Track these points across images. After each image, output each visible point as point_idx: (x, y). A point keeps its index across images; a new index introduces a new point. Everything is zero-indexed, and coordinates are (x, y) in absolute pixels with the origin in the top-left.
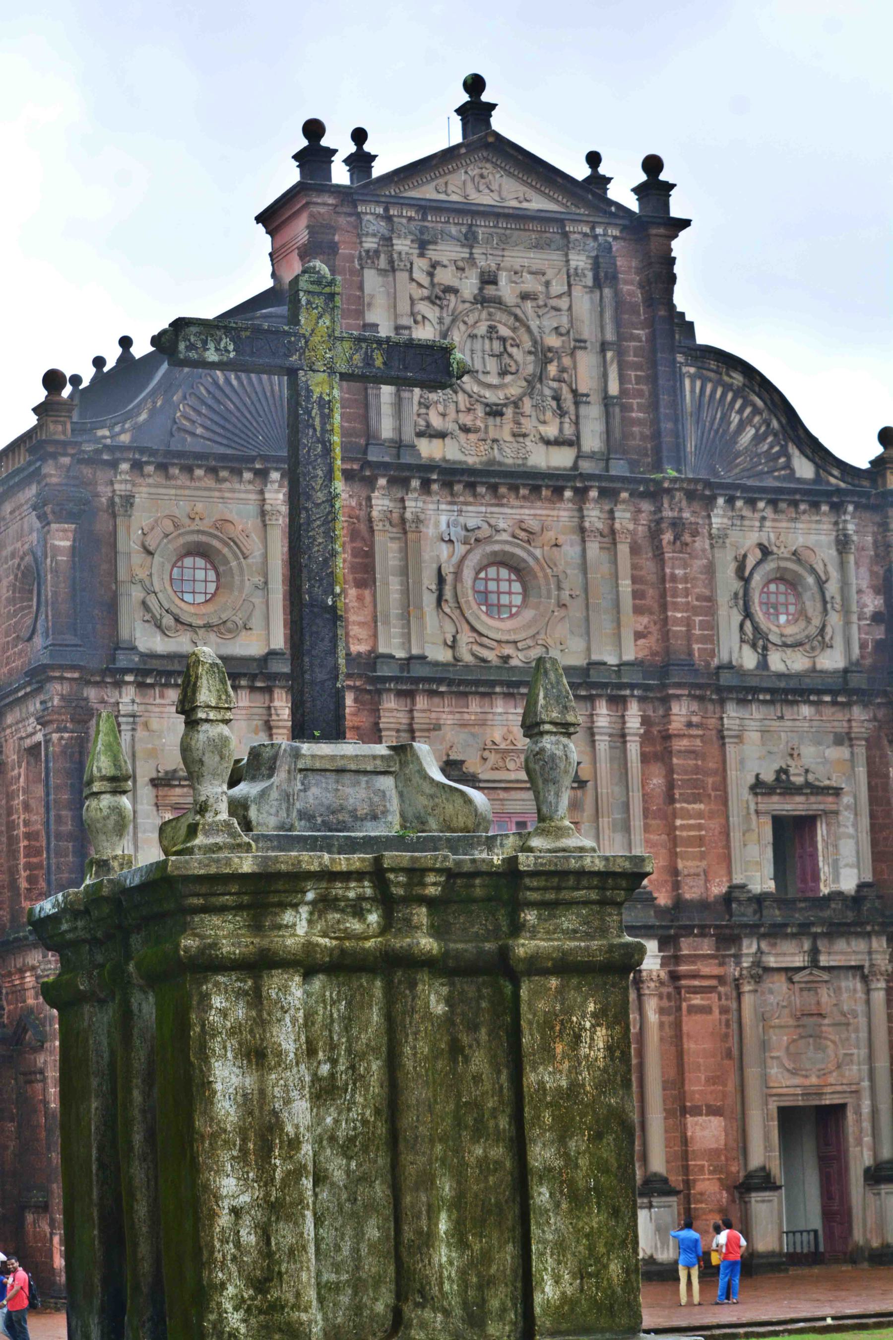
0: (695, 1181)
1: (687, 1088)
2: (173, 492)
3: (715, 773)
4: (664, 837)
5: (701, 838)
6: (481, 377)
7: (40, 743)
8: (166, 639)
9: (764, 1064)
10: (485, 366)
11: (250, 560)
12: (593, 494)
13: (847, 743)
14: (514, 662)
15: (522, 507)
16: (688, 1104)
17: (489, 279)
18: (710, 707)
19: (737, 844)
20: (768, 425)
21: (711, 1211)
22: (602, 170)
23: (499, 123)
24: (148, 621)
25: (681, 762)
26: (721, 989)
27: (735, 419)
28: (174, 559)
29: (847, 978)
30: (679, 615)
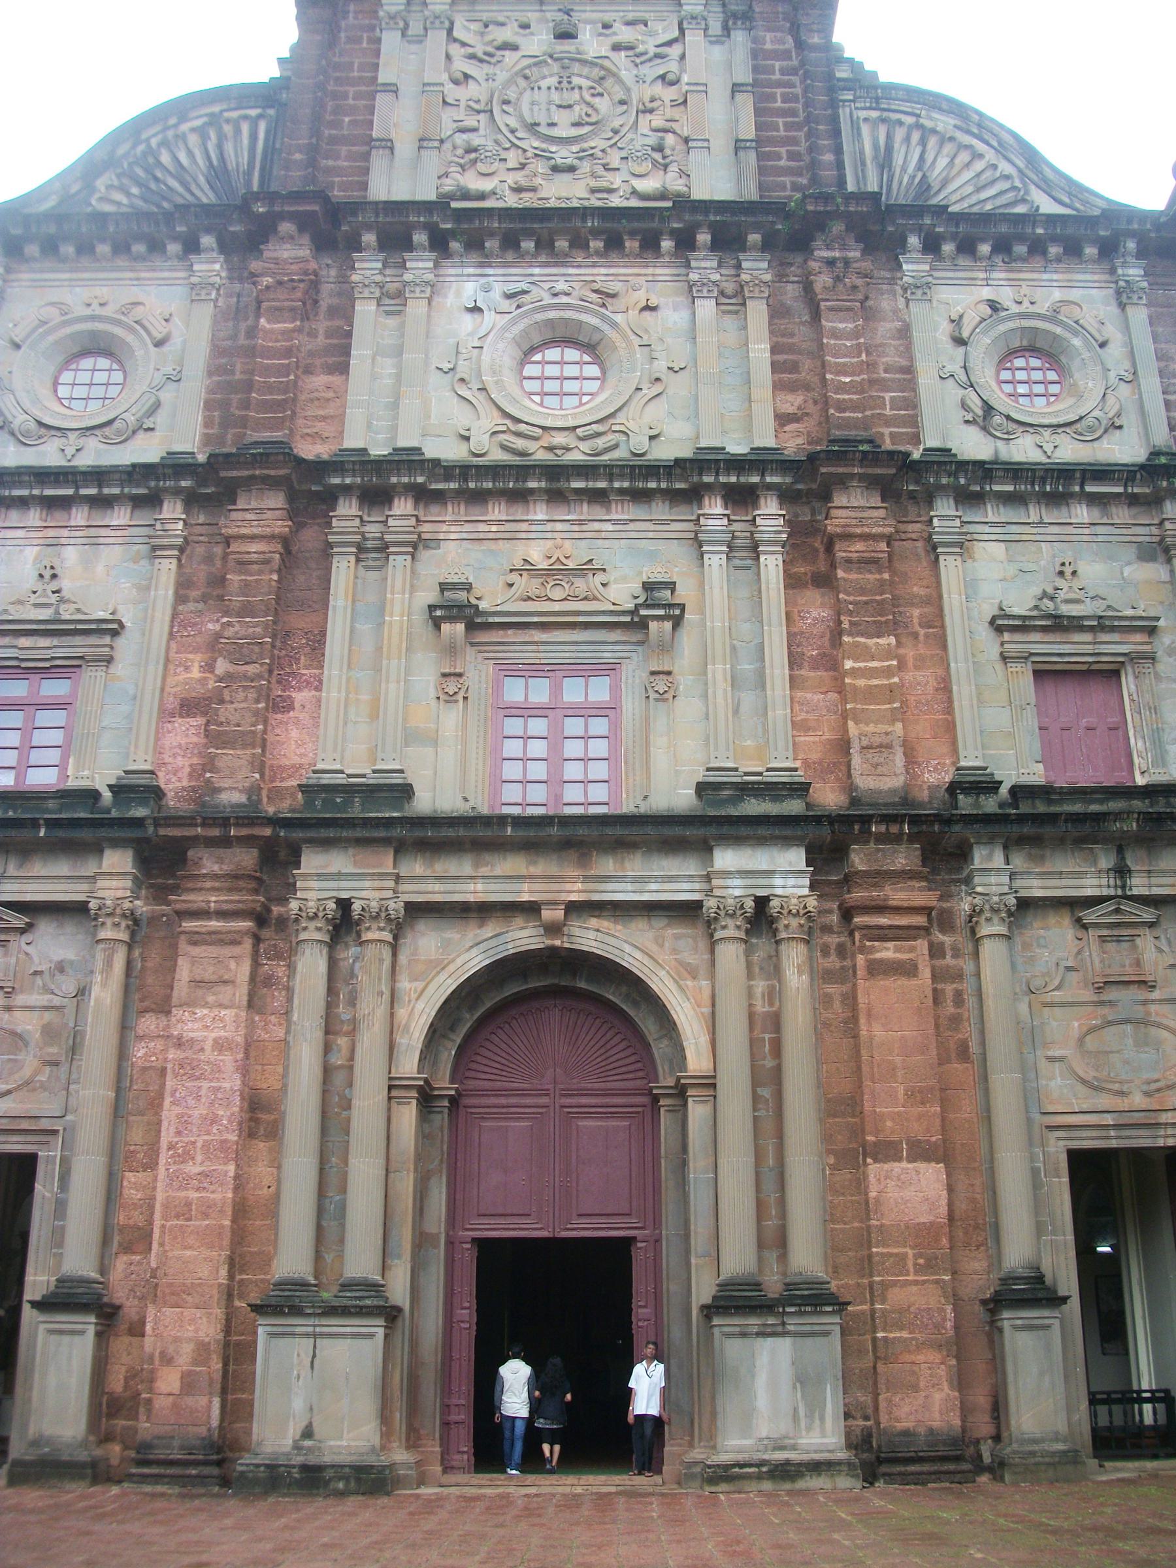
0: (885, 1286)
2: (67, 276)
3: (926, 601)
4: (833, 696)
5: (891, 689)
6: (543, 129)
8: (23, 448)
9: (1027, 1073)
10: (550, 117)
11: (166, 348)
12: (704, 238)
13: (1161, 557)
14: (575, 457)
16: (870, 1138)
17: (565, 35)
18: (912, 510)
19: (965, 703)
20: (995, 167)
21: (921, 1347)
25: (853, 576)
26: (947, 939)
27: (942, 162)
28: (60, 359)
30: (848, 380)
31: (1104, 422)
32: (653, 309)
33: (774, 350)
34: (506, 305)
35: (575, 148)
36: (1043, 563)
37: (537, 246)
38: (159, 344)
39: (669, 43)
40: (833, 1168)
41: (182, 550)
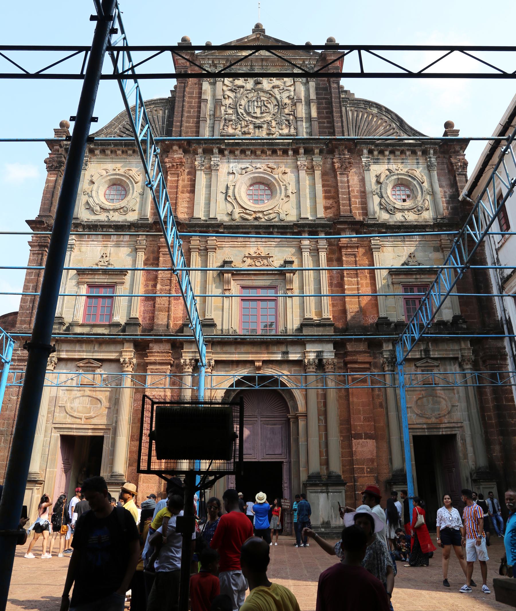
1: (352, 423)
12: (302, 151)
14: (263, 220)
15: (269, 159)
20: (390, 125)
24: (87, 209)
29: (451, 365)
32: (286, 173)
33: (323, 186)
35: (262, 120)
36: (405, 253)
37: (251, 153)
39: (290, 86)
40: (342, 441)
41: (145, 249)
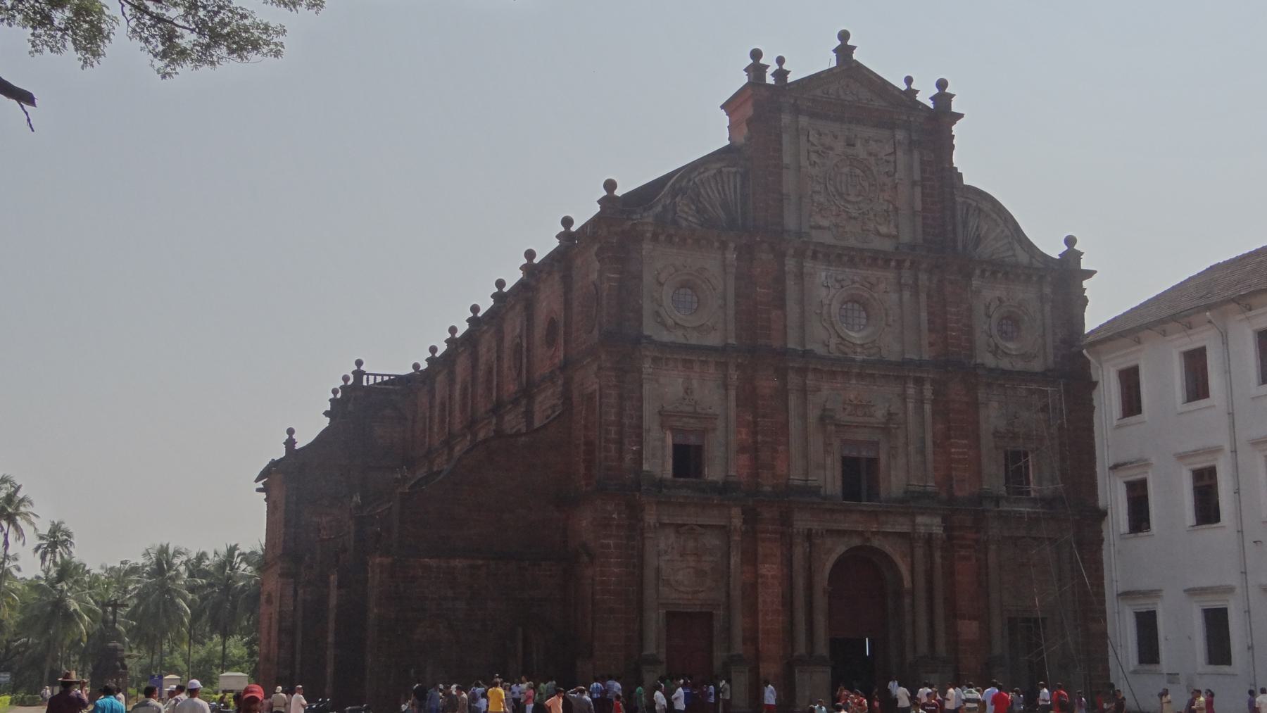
7: (595, 390)
12: (907, 264)
15: (868, 270)
17: (850, 144)
20: (1003, 231)
22: (913, 86)
23: (856, 56)
30: (954, 334)
31: (1033, 355)
34: (837, 285)
38: (714, 289)
